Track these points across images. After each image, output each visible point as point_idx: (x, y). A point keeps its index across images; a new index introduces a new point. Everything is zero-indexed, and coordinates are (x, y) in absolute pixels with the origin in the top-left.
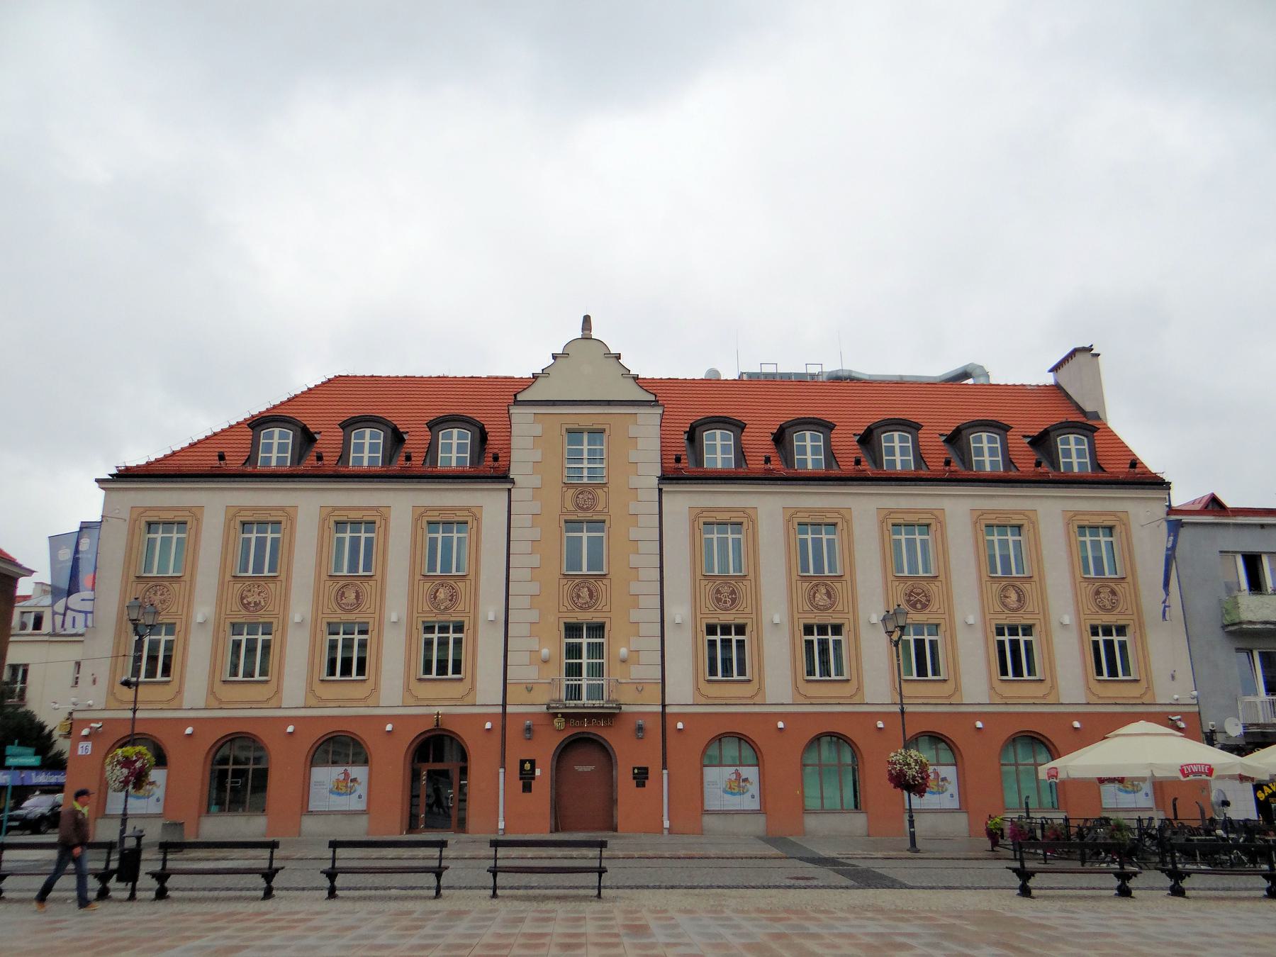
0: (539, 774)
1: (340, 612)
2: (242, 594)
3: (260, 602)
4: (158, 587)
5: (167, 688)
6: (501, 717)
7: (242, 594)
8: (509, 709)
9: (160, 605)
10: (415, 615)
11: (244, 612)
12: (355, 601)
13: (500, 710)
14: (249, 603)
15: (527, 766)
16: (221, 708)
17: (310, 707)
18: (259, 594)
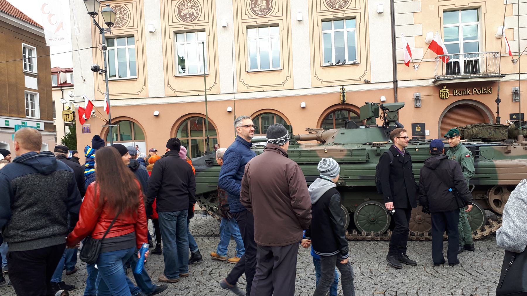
0: (428, 134)
1: (255, 17)
2: (179, 8)
3: (193, 13)
4: (117, 8)
5: (135, 83)
6: (392, 92)
7: (179, 8)
8: (400, 84)
9: (120, 21)
10: (315, 14)
11: (182, 23)
12: (266, 7)
13: (391, 85)
14: (185, 15)
15: (418, 129)
16: (177, 96)
17: (242, 93)
18: (192, 8)
